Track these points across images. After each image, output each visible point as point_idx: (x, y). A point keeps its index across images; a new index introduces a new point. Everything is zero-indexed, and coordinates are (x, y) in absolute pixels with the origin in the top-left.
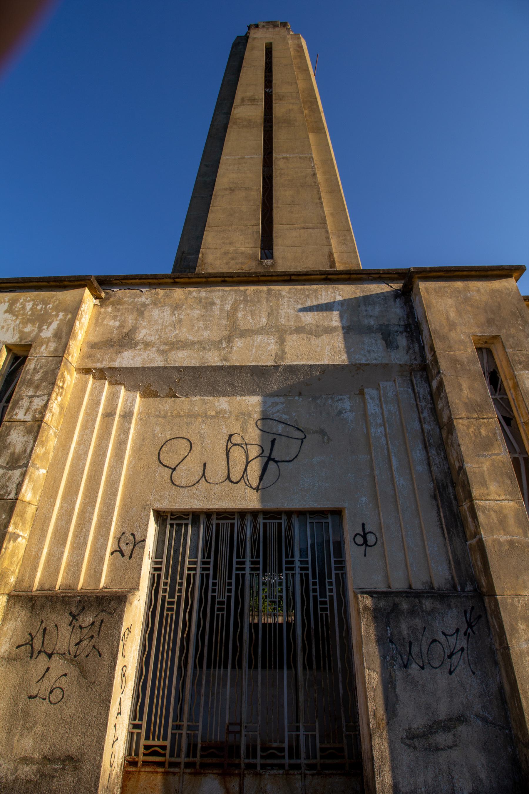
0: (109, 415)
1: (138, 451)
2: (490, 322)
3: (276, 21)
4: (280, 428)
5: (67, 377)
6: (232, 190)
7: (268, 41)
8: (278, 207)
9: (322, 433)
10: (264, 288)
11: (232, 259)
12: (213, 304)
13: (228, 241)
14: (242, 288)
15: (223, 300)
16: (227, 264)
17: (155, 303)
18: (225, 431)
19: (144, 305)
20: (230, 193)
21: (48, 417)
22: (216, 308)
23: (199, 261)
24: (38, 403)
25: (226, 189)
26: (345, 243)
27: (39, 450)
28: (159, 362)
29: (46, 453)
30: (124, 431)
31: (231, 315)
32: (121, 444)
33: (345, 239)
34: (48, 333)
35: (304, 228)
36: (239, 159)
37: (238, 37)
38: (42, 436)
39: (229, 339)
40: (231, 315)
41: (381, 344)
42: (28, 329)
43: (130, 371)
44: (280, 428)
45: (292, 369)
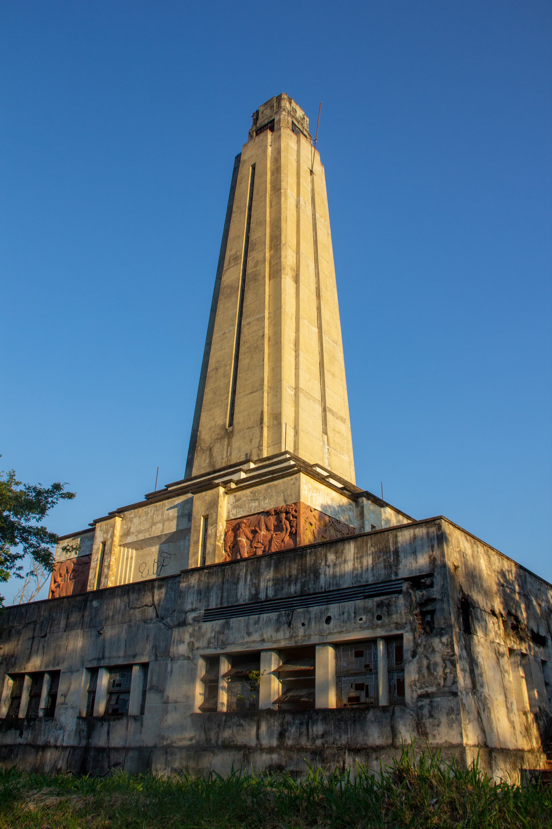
0: (127, 559)
1: (135, 568)
2: (208, 509)
3: (272, 98)
4: (166, 555)
5: (115, 549)
6: (217, 369)
7: (252, 163)
8: (240, 377)
9: (175, 554)
10: (161, 503)
11: (214, 432)
12: (148, 513)
13: (212, 418)
14: (156, 504)
15: (151, 510)
16: (211, 437)
17: (135, 516)
18: (154, 559)
19: (132, 518)
20: (216, 372)
21: (111, 563)
22: (149, 515)
23: (198, 438)
24: (109, 559)
25: (213, 370)
26: (276, 396)
27: (110, 573)
28: (135, 539)
29: (113, 573)
30: (131, 563)
31: (152, 517)
32: (131, 567)
33: (277, 392)
34: (109, 537)
35: (251, 393)
36: (223, 334)
37: (236, 158)
38: (111, 569)
39: (151, 527)
40: (152, 517)
41: (187, 520)
42: (105, 536)
43: (130, 543)
44: (166, 555)
45: (166, 535)
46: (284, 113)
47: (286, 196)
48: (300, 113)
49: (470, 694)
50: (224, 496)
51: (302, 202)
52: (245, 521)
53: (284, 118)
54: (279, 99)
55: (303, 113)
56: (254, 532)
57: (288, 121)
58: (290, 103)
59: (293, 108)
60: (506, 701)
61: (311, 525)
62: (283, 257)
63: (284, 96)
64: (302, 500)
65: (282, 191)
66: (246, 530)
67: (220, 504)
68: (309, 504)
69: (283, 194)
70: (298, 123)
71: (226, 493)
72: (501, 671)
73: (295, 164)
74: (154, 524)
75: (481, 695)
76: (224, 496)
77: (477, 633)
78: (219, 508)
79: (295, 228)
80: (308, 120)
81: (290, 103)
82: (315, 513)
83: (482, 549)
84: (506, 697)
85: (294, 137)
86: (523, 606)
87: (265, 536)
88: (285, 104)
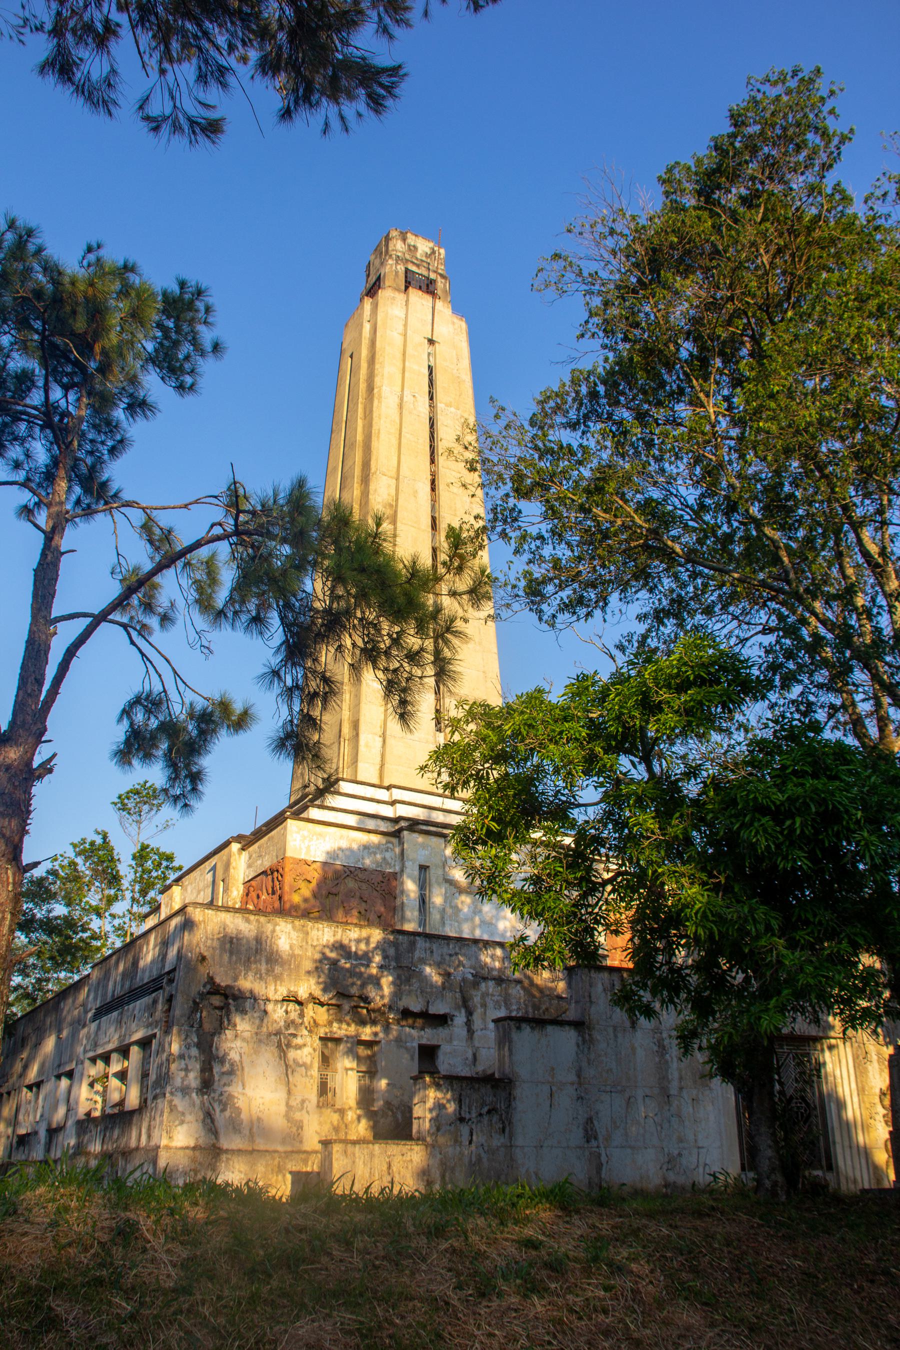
46: (390, 262)
47: (380, 397)
48: (423, 246)
49: (194, 1095)
50: (240, 854)
51: (407, 398)
52: (253, 883)
53: (393, 270)
54: (388, 239)
55: (431, 245)
56: (258, 897)
57: (397, 273)
58: (404, 240)
59: (409, 246)
60: (289, 1099)
61: (309, 882)
62: (371, 492)
63: (394, 233)
64: (289, 853)
65: (376, 391)
66: (253, 894)
67: (233, 864)
68: (303, 857)
69: (376, 395)
70: (418, 266)
71: (243, 849)
72: (287, 1066)
73: (399, 340)
74: (199, 892)
75: (221, 1094)
76: (240, 854)
77: (235, 1025)
78: (232, 870)
79: (395, 442)
80: (442, 251)
81: (404, 240)
82: (314, 866)
83: (290, 926)
84: (289, 1092)
85: (401, 297)
86: (387, 981)
87: (264, 901)
88: (398, 246)
